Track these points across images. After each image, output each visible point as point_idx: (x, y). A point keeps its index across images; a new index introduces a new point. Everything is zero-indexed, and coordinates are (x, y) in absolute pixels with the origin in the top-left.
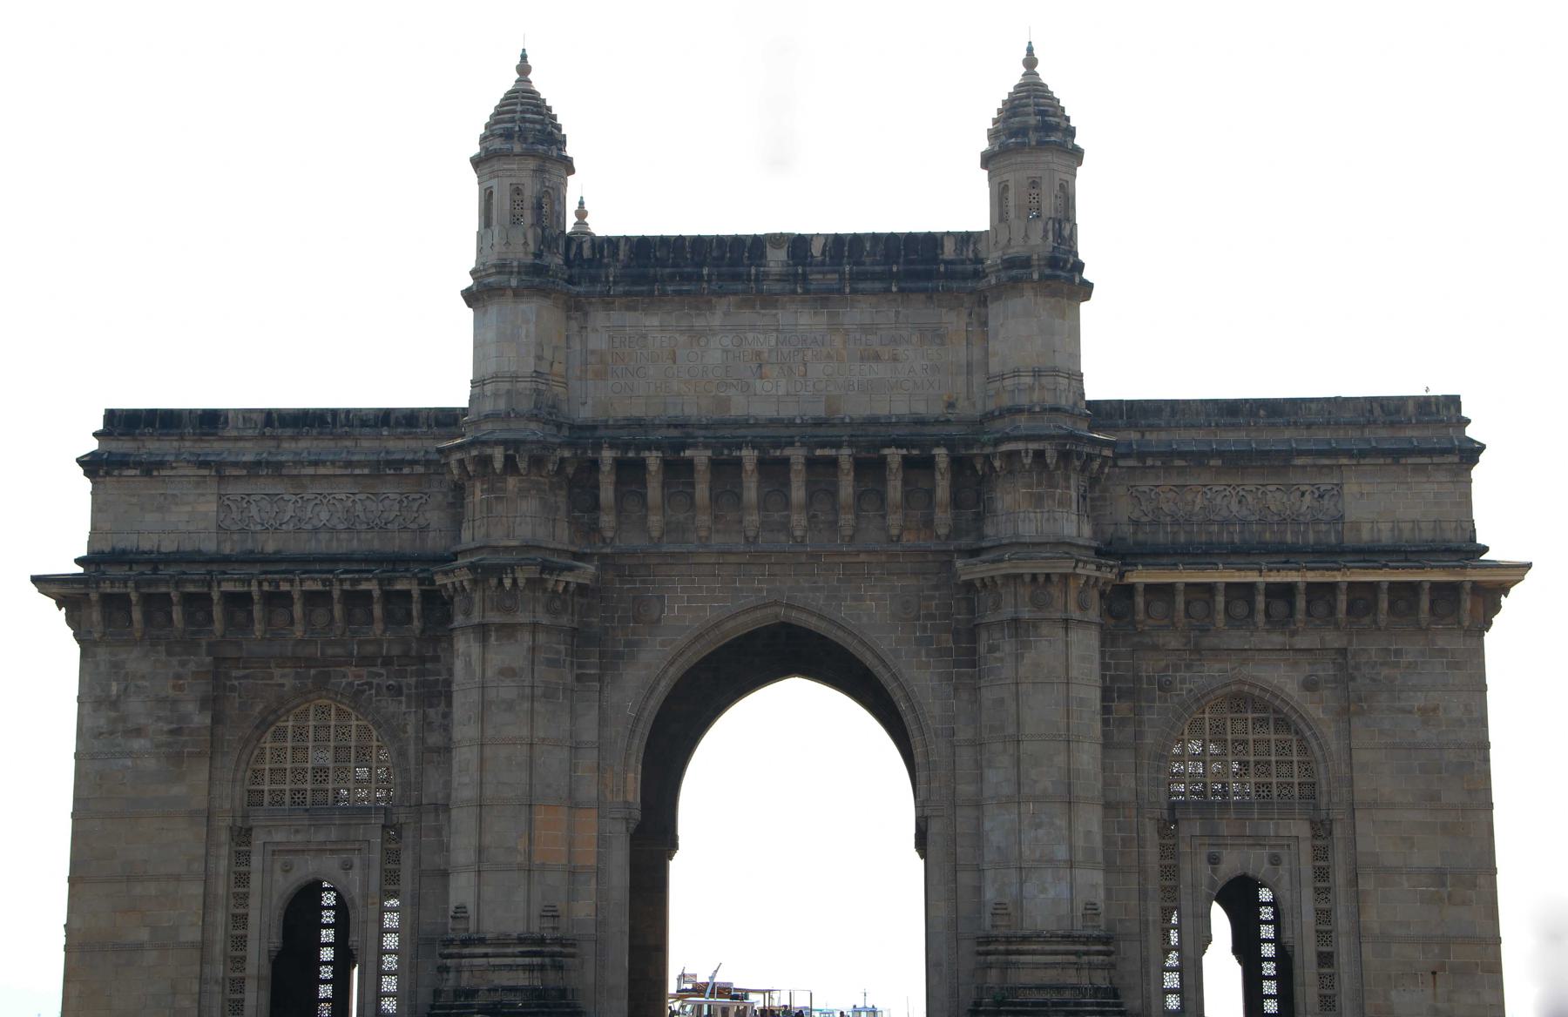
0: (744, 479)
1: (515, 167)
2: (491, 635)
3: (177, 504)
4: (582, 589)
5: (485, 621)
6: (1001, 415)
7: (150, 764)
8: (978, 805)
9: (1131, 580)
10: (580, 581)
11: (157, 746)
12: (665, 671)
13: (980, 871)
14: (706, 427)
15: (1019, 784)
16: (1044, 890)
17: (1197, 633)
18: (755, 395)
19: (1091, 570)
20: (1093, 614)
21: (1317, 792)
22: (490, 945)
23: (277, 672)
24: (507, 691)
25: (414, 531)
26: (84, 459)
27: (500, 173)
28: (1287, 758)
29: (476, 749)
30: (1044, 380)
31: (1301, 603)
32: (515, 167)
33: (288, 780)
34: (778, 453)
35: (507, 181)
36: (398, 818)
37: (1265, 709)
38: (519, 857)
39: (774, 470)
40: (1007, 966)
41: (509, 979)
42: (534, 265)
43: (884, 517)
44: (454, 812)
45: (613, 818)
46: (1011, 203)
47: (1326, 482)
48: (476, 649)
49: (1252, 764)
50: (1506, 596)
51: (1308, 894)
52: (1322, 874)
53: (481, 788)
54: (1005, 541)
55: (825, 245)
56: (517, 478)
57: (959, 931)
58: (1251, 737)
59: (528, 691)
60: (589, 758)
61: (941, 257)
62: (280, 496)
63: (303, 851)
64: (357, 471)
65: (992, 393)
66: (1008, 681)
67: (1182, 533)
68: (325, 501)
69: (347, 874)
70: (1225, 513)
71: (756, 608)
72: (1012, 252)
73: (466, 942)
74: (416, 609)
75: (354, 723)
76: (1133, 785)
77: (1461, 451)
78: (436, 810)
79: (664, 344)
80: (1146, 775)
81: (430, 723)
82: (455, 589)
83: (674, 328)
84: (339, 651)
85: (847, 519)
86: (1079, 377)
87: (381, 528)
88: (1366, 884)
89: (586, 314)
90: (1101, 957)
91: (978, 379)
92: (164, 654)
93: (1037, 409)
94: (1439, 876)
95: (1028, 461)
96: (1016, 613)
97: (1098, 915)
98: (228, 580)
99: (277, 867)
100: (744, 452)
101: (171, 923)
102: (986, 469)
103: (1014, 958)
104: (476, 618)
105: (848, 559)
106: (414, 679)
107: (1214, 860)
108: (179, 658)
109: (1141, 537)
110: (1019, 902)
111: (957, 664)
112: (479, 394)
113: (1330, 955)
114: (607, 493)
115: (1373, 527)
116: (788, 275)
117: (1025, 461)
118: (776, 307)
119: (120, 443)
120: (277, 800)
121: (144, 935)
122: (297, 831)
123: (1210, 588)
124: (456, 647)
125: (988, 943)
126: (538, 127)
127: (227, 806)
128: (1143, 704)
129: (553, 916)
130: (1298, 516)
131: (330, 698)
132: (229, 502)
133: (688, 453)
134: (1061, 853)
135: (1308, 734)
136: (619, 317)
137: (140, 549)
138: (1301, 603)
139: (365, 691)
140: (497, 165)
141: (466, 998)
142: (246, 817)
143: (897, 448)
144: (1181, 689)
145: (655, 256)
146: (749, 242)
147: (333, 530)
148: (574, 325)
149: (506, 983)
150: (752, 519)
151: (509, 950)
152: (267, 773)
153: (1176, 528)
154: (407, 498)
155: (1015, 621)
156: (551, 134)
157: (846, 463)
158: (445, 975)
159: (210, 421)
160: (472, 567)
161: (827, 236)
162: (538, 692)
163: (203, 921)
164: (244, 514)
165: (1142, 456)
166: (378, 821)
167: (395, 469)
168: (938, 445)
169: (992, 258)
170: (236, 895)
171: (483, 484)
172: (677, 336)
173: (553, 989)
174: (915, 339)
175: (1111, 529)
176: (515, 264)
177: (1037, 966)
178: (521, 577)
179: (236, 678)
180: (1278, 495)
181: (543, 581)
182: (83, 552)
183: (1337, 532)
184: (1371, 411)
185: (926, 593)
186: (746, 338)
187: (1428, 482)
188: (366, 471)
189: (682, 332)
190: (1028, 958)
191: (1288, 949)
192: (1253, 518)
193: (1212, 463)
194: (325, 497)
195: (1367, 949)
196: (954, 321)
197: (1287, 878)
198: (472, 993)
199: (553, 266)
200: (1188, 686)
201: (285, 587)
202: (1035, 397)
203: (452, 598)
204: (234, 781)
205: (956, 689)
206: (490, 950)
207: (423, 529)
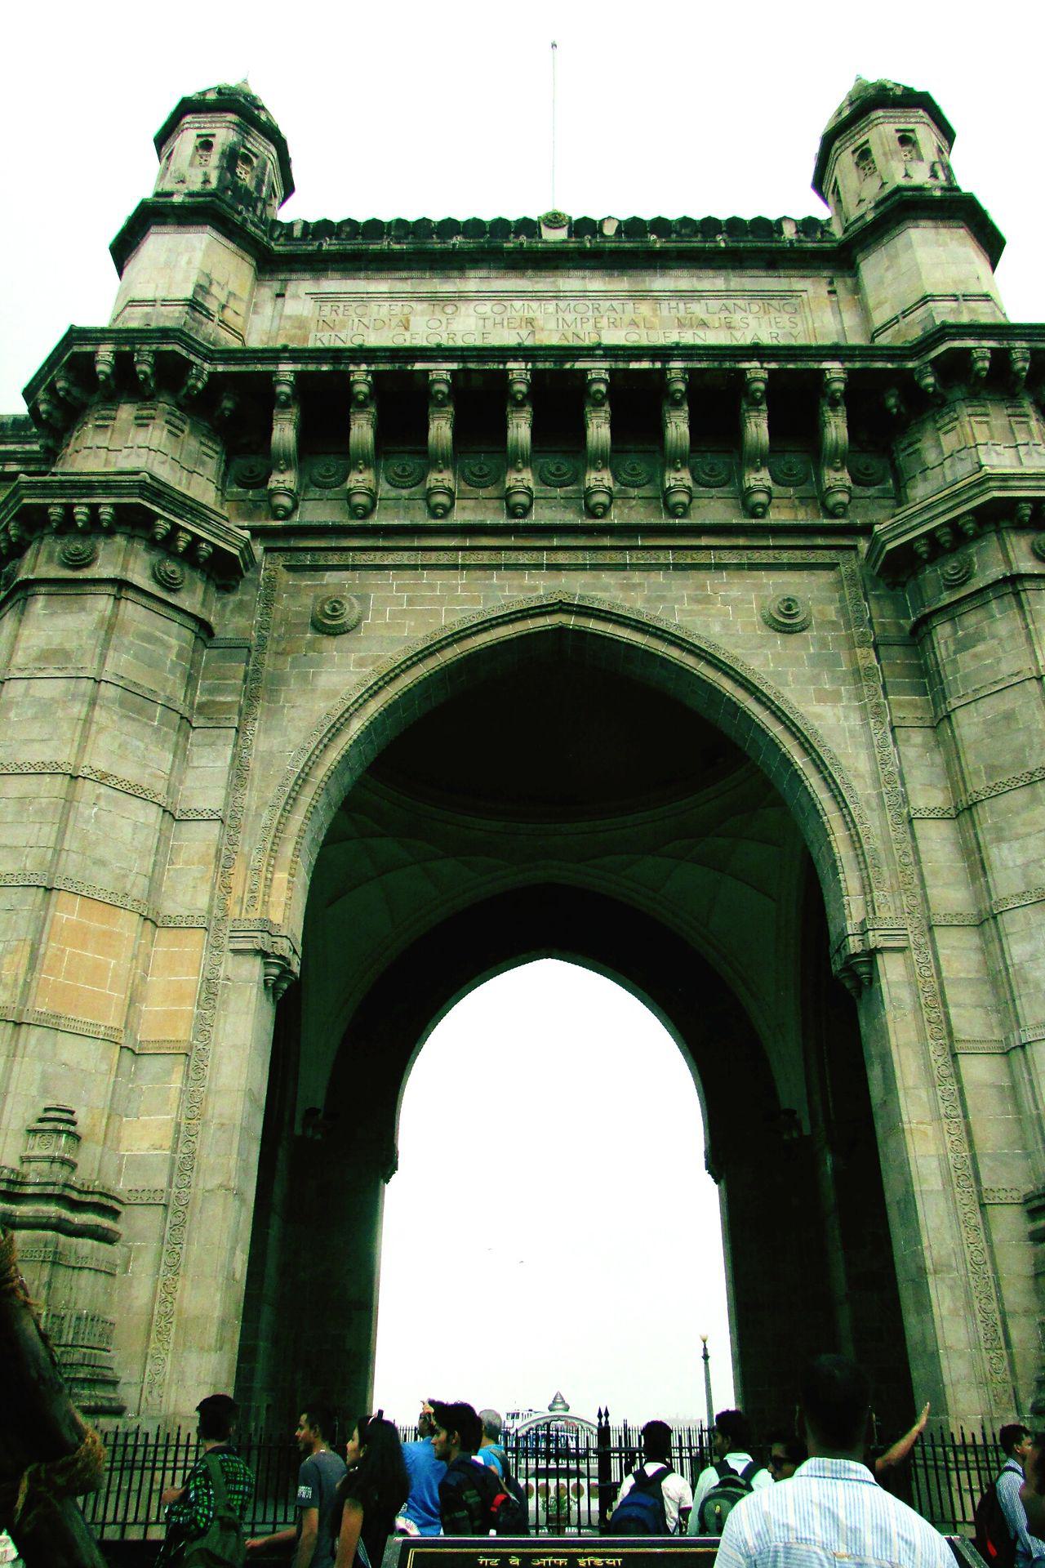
2: (36, 600)
12: (360, 704)
30: (972, 304)
34: (568, 366)
35: (195, 133)
45: (233, 951)
55: (619, 227)
57: (985, 1184)
59: (86, 686)
60: (201, 839)
66: (1016, 679)
79: (393, 312)
83: (410, 295)
100: (510, 365)
102: (903, 409)
114: (284, 433)
133: (418, 366)
136: (332, 284)
140: (188, 118)
172: (413, 304)
189: (420, 300)
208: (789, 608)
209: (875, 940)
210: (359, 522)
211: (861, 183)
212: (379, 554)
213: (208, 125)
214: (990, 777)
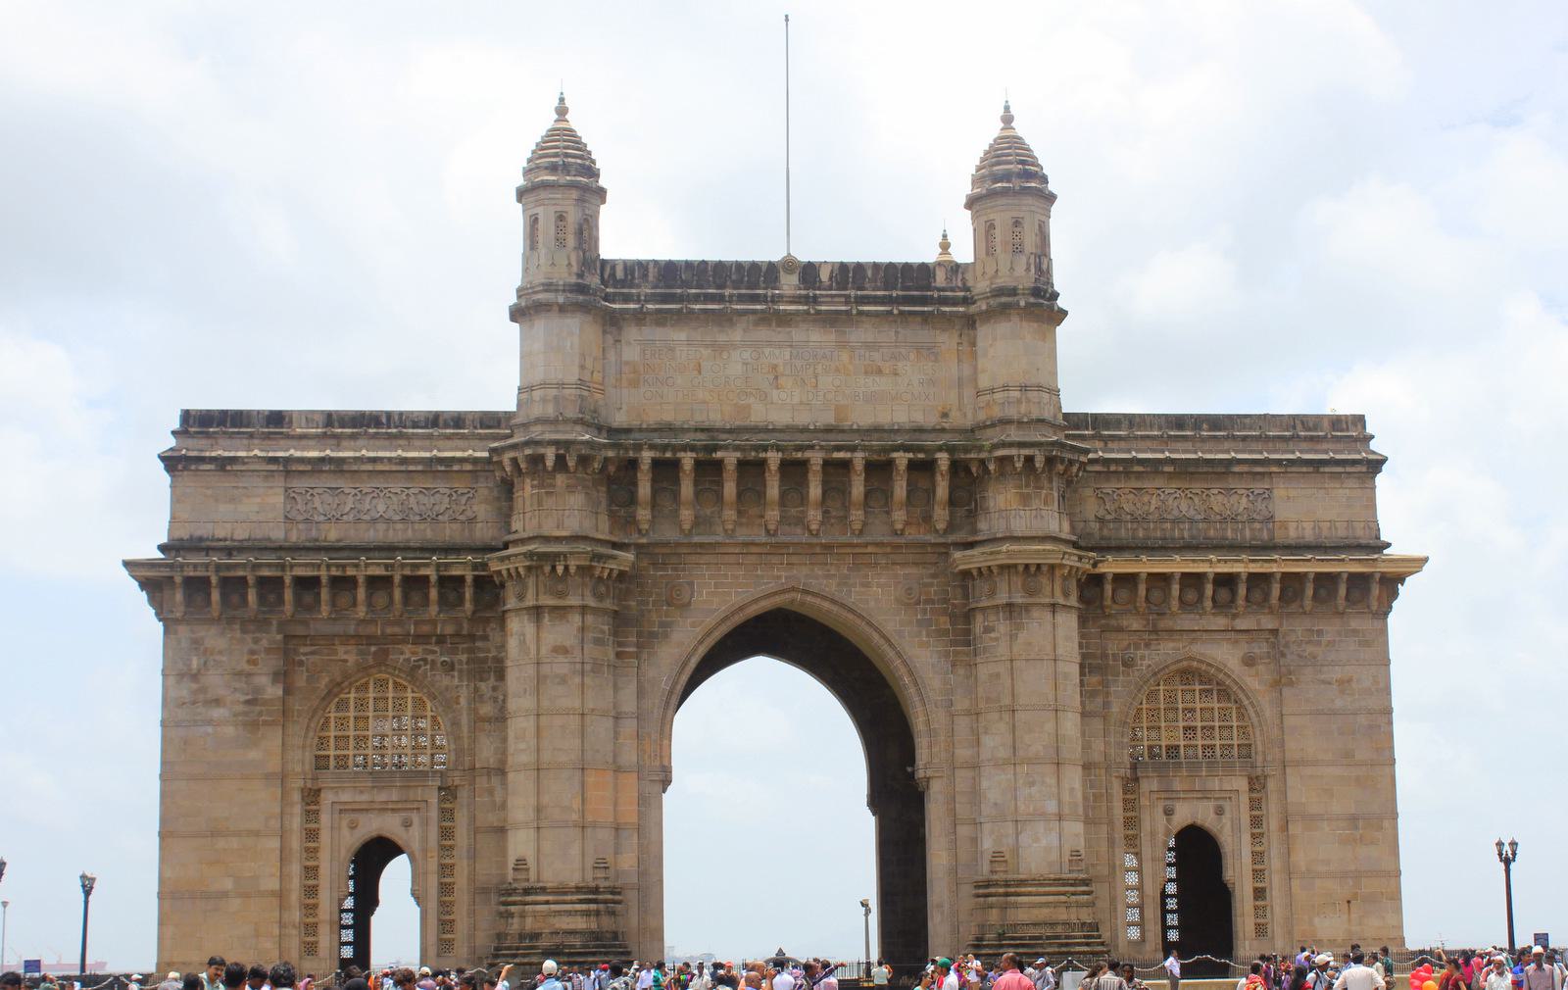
0: (768, 478)
1: (559, 196)
2: (544, 617)
3: (248, 497)
4: (622, 575)
5: (540, 603)
6: (993, 425)
7: (230, 731)
8: (975, 766)
9: (1103, 570)
10: (622, 568)
11: (236, 715)
12: (695, 649)
13: (976, 824)
14: (730, 431)
15: (1014, 748)
16: (1037, 840)
17: (1155, 616)
18: (772, 403)
19: (1072, 561)
20: (1073, 601)
21: (1253, 751)
22: (550, 894)
23: (341, 649)
24: (561, 666)
25: (463, 522)
26: (166, 455)
27: (546, 202)
28: (1228, 723)
29: (532, 719)
30: (1031, 395)
31: (1242, 591)
32: (559, 196)
33: (351, 747)
35: (552, 209)
36: (453, 781)
37: (1210, 682)
38: (574, 815)
39: (794, 470)
40: (1004, 908)
41: (568, 924)
42: (578, 285)
43: (888, 513)
44: (511, 776)
46: (998, 240)
47: (1259, 486)
48: (530, 629)
49: (1200, 729)
50: (1402, 585)
51: (1246, 838)
52: (1256, 821)
53: (538, 754)
54: (999, 535)
55: (832, 272)
56: (564, 475)
58: (1198, 706)
59: (578, 666)
60: (629, 726)
61: (933, 285)
62: (339, 491)
63: (367, 810)
64: (411, 468)
65: (982, 405)
67: (1141, 529)
68: (382, 495)
69: (407, 831)
70: (1176, 512)
71: (775, 593)
72: (1000, 282)
73: (527, 892)
74: (468, 593)
75: (410, 695)
76: (1102, 749)
77: (1369, 462)
78: (489, 775)
80: (1112, 740)
81: (481, 696)
82: (509, 574)
84: (397, 630)
85: (857, 515)
86: (1055, 392)
87: (433, 519)
88: (1295, 829)
89: (620, 329)
90: (1086, 897)
91: (968, 392)
92: (239, 631)
93: (1025, 420)
94: (1353, 820)
95: (1019, 465)
96: (1010, 598)
97: (1081, 860)
98: (300, 565)
99: (344, 823)
101: (252, 874)
102: (980, 472)
103: (1012, 899)
104: (530, 601)
105: (857, 550)
106: (465, 656)
107: (1169, 812)
108: (251, 635)
109: (1105, 532)
110: (1016, 850)
111: (954, 643)
112: (528, 399)
113: (1263, 890)
114: (644, 489)
115: (1298, 527)
116: (800, 296)
117: (1017, 465)
118: (790, 326)
119: (195, 440)
120: (342, 762)
121: (228, 884)
122: (361, 792)
123: (1164, 579)
124: (509, 627)
125: (987, 886)
126: (579, 161)
127: (298, 769)
128: (1110, 678)
129: (605, 868)
130: (1236, 515)
131: (389, 673)
132: (293, 495)
133: (719, 455)
134: (1051, 807)
135: (1246, 702)
137: (216, 537)
138: (1242, 591)
139: (419, 667)
140: (543, 194)
141: (531, 939)
142: (315, 779)
143: (905, 452)
144: (1141, 665)
145: (681, 277)
146: (764, 269)
147: (389, 521)
148: (610, 339)
149: (565, 927)
150: (773, 514)
151: (569, 898)
152: (332, 740)
153: (1135, 525)
154: (456, 492)
155: (1010, 607)
156: (589, 168)
157: (859, 464)
158: (510, 920)
159: (277, 418)
160: (530, 555)
161: (834, 263)
162: (588, 667)
163: (281, 872)
164: (310, 505)
165: (1107, 462)
166: (434, 784)
167: (446, 466)
168: (940, 449)
169: (981, 286)
170: (307, 850)
171: (532, 480)
172: (701, 349)
173: (607, 932)
174: (912, 356)
175: (1082, 525)
176: (561, 283)
177: (1033, 906)
178: (573, 563)
179: (303, 654)
180: (1220, 498)
181: (591, 568)
182: (164, 539)
183: (1268, 529)
184: (1294, 427)
185: (925, 580)
186: (763, 352)
187: (1341, 488)
188: (420, 468)
189: (707, 346)
191: (1229, 886)
192: (1199, 517)
193: (1167, 469)
194: (381, 491)
195: (1295, 883)
196: (947, 340)
197: (1229, 824)
198: (536, 936)
199: (593, 286)
200: (1146, 662)
201: (350, 572)
202: (1023, 410)
203: (502, 586)
204: (304, 747)
205: (953, 665)
206: (550, 898)
207: (472, 520)
208: (909, 594)
209: (929, 773)
210: (685, 541)
211: (987, 254)
212: (698, 556)
213: (561, 202)
214: (987, 703)
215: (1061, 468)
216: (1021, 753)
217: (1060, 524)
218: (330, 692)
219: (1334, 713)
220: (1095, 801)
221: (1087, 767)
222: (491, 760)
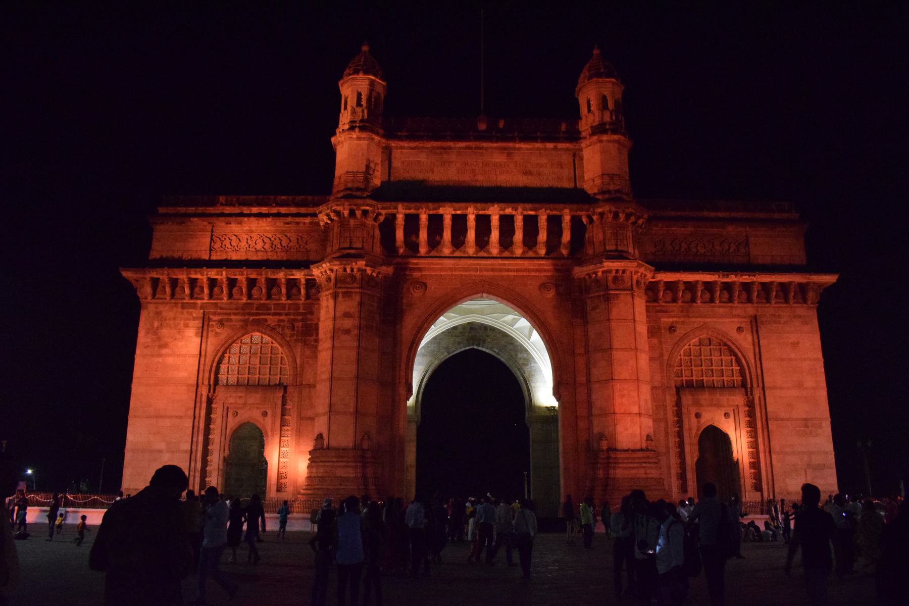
20: (642, 291)
24: (348, 323)
29: (330, 352)
44: (318, 386)
94: (806, 420)
106: (301, 323)
107: (698, 416)
110: (613, 436)
121: (163, 446)
122: (240, 397)
127: (206, 383)
134: (635, 410)
135: (740, 355)
181: (365, 270)
190: (621, 465)
195: (774, 456)
207: (308, 251)
215: (633, 219)
216: (616, 377)
217: (634, 252)
218: (225, 342)
219: (790, 360)
220: (657, 409)
221: (653, 388)
222: (312, 381)
